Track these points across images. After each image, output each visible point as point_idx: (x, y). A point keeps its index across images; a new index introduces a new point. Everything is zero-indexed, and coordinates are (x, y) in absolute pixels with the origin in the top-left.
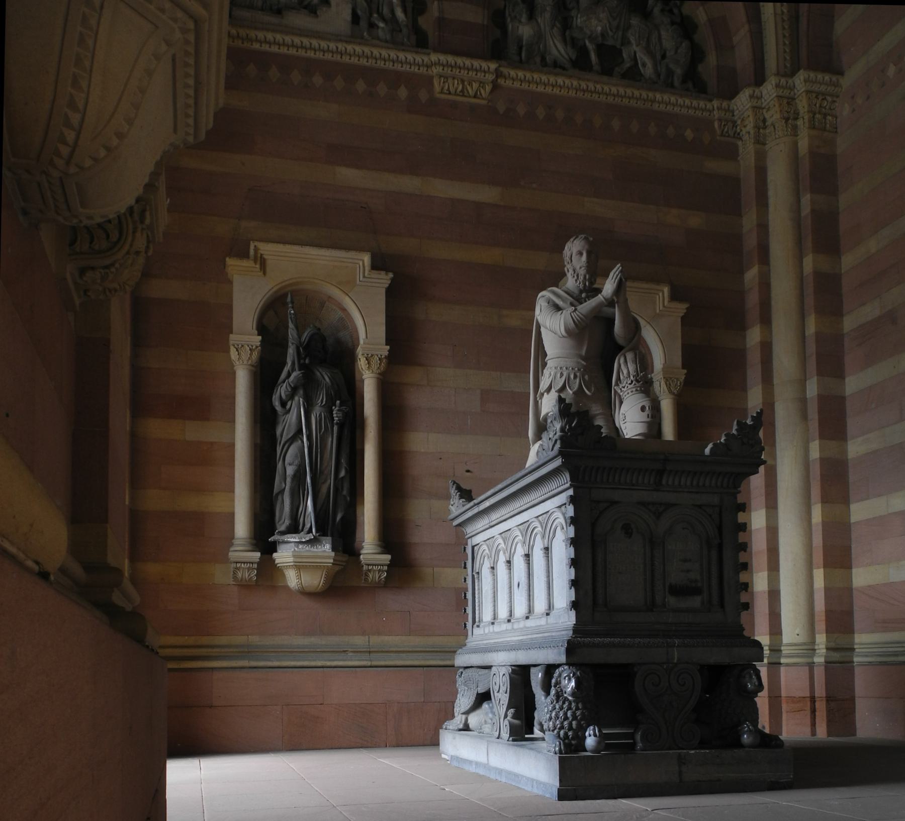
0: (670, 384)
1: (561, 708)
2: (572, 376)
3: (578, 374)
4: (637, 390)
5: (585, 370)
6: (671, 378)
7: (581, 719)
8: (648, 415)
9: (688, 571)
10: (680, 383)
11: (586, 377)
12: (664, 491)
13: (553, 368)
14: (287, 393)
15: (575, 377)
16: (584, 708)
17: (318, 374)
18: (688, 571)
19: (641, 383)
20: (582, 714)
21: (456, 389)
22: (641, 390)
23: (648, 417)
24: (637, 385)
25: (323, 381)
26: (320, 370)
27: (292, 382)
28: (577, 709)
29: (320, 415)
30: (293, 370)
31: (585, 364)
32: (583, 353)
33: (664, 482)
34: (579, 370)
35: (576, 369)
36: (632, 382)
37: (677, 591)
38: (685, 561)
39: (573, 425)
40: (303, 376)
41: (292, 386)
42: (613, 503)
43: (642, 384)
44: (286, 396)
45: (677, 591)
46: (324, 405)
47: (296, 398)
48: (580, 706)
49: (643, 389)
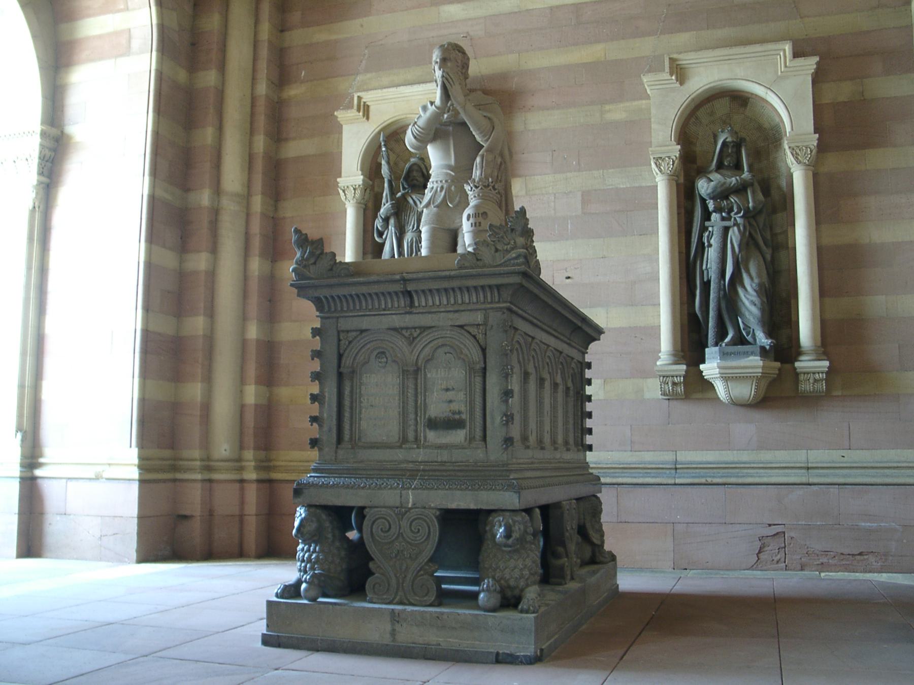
0: (797, 154)
1: (308, 550)
2: (439, 189)
3: (445, 186)
4: (475, 197)
5: (452, 181)
6: (798, 147)
7: (315, 563)
8: (472, 224)
9: (450, 401)
10: (811, 151)
11: (453, 188)
12: (416, 313)
13: (435, 183)
14: (381, 224)
15: (442, 188)
16: (321, 551)
17: (411, 201)
18: (450, 401)
19: (480, 188)
20: (317, 557)
21: (555, 194)
22: (479, 195)
23: (472, 226)
24: (477, 190)
25: (415, 207)
26: (414, 197)
27: (382, 214)
28: (314, 551)
29: (412, 239)
30: (387, 202)
31: (453, 174)
32: (453, 162)
33: (417, 304)
34: (446, 181)
35: (444, 181)
36: (472, 188)
37: (433, 424)
38: (447, 390)
39: (305, 256)
40: (392, 207)
41: (383, 217)
42: (362, 331)
43: (481, 188)
44: (381, 227)
45: (433, 424)
46: (416, 230)
47: (390, 227)
48: (317, 548)
49: (481, 195)
